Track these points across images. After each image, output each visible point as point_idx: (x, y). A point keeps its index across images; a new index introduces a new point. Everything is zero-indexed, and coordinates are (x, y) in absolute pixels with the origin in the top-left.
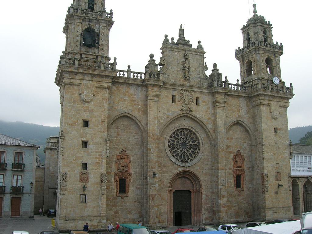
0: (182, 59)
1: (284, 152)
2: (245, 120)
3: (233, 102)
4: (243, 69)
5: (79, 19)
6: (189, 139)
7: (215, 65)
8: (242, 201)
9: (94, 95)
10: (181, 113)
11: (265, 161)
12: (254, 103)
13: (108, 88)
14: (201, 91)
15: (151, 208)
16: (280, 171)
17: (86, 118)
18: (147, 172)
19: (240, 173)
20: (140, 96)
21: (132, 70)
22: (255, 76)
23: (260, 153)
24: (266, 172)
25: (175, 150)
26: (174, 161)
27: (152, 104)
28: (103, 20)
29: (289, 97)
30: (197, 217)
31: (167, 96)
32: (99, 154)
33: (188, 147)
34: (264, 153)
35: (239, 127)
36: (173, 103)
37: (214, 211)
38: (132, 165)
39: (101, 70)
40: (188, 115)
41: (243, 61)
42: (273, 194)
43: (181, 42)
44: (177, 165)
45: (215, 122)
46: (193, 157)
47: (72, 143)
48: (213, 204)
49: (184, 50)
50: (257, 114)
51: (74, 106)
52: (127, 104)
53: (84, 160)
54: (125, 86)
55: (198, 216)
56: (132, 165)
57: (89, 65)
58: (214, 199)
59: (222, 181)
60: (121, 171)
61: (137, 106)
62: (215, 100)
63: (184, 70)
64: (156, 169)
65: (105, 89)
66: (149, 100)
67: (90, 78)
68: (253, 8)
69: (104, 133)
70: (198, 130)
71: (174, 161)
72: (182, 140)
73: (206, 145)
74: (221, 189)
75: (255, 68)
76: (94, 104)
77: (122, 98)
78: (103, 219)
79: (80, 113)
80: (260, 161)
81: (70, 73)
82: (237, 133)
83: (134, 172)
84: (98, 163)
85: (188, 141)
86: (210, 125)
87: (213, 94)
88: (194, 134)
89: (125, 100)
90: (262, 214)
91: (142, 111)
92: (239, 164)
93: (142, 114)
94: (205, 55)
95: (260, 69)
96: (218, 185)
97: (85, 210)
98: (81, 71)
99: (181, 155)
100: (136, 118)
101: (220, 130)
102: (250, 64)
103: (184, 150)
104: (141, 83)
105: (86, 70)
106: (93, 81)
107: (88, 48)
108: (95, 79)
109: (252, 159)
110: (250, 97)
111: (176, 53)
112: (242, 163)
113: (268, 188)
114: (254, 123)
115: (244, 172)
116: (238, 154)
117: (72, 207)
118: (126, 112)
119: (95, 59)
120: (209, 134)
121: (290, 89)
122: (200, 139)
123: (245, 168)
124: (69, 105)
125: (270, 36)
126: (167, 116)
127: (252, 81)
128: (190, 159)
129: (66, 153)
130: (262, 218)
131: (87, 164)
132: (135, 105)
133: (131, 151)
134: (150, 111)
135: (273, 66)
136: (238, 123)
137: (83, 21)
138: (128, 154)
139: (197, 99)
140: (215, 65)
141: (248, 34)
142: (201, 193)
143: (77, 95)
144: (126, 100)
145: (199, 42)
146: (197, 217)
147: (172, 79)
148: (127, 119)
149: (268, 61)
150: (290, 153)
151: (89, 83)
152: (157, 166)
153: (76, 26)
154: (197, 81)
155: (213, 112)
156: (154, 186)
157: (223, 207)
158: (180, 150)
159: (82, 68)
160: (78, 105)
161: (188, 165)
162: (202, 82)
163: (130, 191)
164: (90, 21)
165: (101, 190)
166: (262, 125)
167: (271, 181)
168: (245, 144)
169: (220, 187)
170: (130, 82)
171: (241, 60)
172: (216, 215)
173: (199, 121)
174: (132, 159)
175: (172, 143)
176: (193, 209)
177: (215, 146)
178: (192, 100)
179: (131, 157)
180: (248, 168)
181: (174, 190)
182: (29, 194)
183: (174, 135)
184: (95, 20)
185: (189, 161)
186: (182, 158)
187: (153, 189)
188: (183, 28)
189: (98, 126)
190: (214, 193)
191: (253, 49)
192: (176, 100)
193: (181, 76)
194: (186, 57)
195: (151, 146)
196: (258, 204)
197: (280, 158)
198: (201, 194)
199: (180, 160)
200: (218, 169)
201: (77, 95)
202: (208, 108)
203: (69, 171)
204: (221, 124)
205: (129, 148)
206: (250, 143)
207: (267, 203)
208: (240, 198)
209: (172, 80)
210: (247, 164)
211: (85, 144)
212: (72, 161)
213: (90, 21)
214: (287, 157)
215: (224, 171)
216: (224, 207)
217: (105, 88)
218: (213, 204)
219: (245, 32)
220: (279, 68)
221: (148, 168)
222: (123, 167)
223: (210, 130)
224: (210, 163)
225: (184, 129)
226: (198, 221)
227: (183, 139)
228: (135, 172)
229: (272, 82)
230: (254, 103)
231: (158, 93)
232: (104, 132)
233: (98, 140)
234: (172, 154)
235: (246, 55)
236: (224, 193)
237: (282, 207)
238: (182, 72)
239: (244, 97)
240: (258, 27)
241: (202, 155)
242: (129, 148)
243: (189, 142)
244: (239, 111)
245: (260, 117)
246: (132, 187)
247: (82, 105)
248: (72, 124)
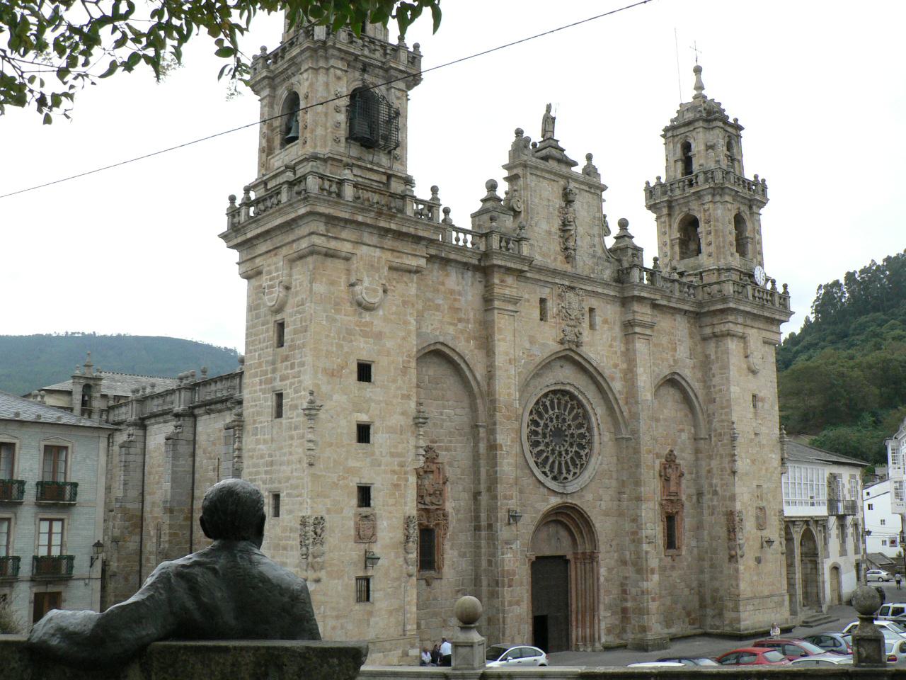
0: (559, 202)
1: (771, 458)
2: (689, 373)
3: (662, 324)
4: (670, 236)
5: (342, 59)
6: (569, 418)
7: (623, 224)
8: (678, 581)
9: (385, 291)
10: (558, 347)
11: (736, 478)
12: (708, 331)
13: (417, 271)
14: (600, 290)
15: (507, 608)
16: (764, 504)
17: (365, 357)
18: (493, 510)
19: (674, 511)
20: (470, 298)
21: (456, 223)
22: (712, 260)
23: (722, 457)
24: (738, 506)
25: (540, 448)
26: (541, 477)
27: (502, 321)
28: (401, 71)
29: (783, 318)
30: (584, 627)
31: (528, 301)
32: (401, 459)
33: (566, 441)
34: (736, 458)
35: (672, 391)
36: (541, 320)
37: (624, 610)
38: (448, 488)
39: (408, 220)
40: (572, 354)
41: (669, 215)
42: (752, 563)
43: (554, 152)
44: (546, 489)
45: (630, 375)
46: (579, 467)
47: (333, 428)
48: (624, 592)
49: (563, 177)
50: (713, 357)
51: (335, 320)
52: (443, 317)
53: (363, 477)
54: (436, 266)
55: (588, 624)
56: (449, 489)
57: (377, 203)
58: (626, 578)
59: (649, 532)
60: (427, 507)
61: (464, 325)
62: (630, 318)
63: (564, 231)
64: (514, 501)
65: (408, 274)
66: (496, 311)
67: (374, 240)
68: (692, 78)
69: (410, 399)
70: (589, 395)
71: (541, 477)
72: (555, 420)
73: (607, 437)
74: (647, 553)
75: (711, 238)
76: (384, 314)
77: (429, 300)
78: (413, 646)
79: (351, 341)
80: (722, 479)
81: (331, 220)
82: (670, 407)
83: (453, 508)
84: (396, 486)
85: (566, 424)
87: (625, 302)
88: (580, 405)
89: (438, 308)
90: (729, 615)
91: (475, 338)
92: (673, 489)
93: (476, 348)
94: (604, 195)
95: (724, 241)
96: (637, 541)
97: (368, 620)
98: (360, 219)
99: (553, 462)
100: (462, 357)
101: (644, 398)
102: (690, 225)
103: (560, 447)
104: (477, 263)
105: (372, 215)
106: (383, 248)
107: (364, 149)
108: (388, 243)
109: (697, 473)
110: (697, 314)
111: (545, 183)
112: (679, 484)
113: (744, 548)
114: (706, 380)
115: (683, 505)
116: (670, 460)
117: (337, 617)
118: (441, 341)
119: (381, 185)
120: (616, 406)
121: (785, 299)
122: (593, 419)
123: (684, 498)
124: (325, 315)
125: (739, 158)
126: (531, 356)
127: (701, 273)
128: (572, 473)
129: (319, 458)
130: (727, 625)
131: (372, 490)
132: (460, 320)
133: (447, 449)
134: (499, 340)
135: (747, 238)
136: (673, 381)
137: (348, 65)
138: (440, 460)
139: (591, 310)
140: (623, 224)
141: (687, 147)
142: (595, 564)
143: (343, 287)
144: (440, 305)
145: (589, 157)
146: (584, 627)
147: (540, 254)
148: (435, 360)
149: (739, 221)
150: (782, 459)
151: (373, 254)
152: (514, 492)
153: (332, 79)
154: (590, 262)
155: (623, 349)
156: (511, 548)
157: (652, 598)
158: (551, 448)
159: (363, 210)
160: (347, 317)
161: (571, 487)
162: (600, 268)
163: (447, 563)
164: (364, 70)
165: (407, 563)
166: (728, 389)
167: (748, 530)
168: (683, 434)
169: (645, 547)
170: (452, 256)
171: (665, 211)
172: (633, 622)
173: (595, 374)
174: (449, 472)
175: (533, 428)
176: (574, 606)
177: (628, 439)
178: (583, 315)
179: (447, 467)
180: (689, 496)
181: (534, 559)
182: (87, 581)
183: (539, 410)
184: (381, 68)
185: (570, 477)
186: (556, 470)
187: (509, 555)
188: (552, 114)
189: (394, 381)
190: (624, 563)
191: (710, 188)
192: (549, 312)
193: (558, 248)
194: (571, 198)
195: (502, 437)
196: (717, 590)
197: (764, 472)
198: (595, 567)
199: (550, 476)
200: (639, 499)
201: (342, 288)
202: (614, 339)
203: (328, 511)
204: (645, 381)
205: (441, 441)
206: (693, 431)
207: (743, 586)
208: (675, 574)
209: (538, 259)
210: (688, 487)
211: (363, 433)
212: (334, 483)
213: (364, 70)
214: (776, 468)
215: (651, 505)
216: (654, 600)
217: (410, 272)
218: (624, 592)
219: (676, 139)
220: (760, 243)
221: (495, 498)
222: (430, 495)
223: (618, 396)
224: (614, 483)
225: (559, 390)
226: (588, 639)
228: (457, 511)
229: (751, 276)
230: (708, 331)
231: (514, 292)
232: (408, 397)
233: (397, 420)
235: (682, 201)
236: (654, 562)
237: (768, 597)
238: (560, 237)
239: (686, 312)
240: (717, 131)
241: (599, 462)
242: (441, 441)
243: (569, 425)
244: (676, 351)
245: (725, 367)
246: (450, 552)
247: (356, 318)
248: (333, 373)
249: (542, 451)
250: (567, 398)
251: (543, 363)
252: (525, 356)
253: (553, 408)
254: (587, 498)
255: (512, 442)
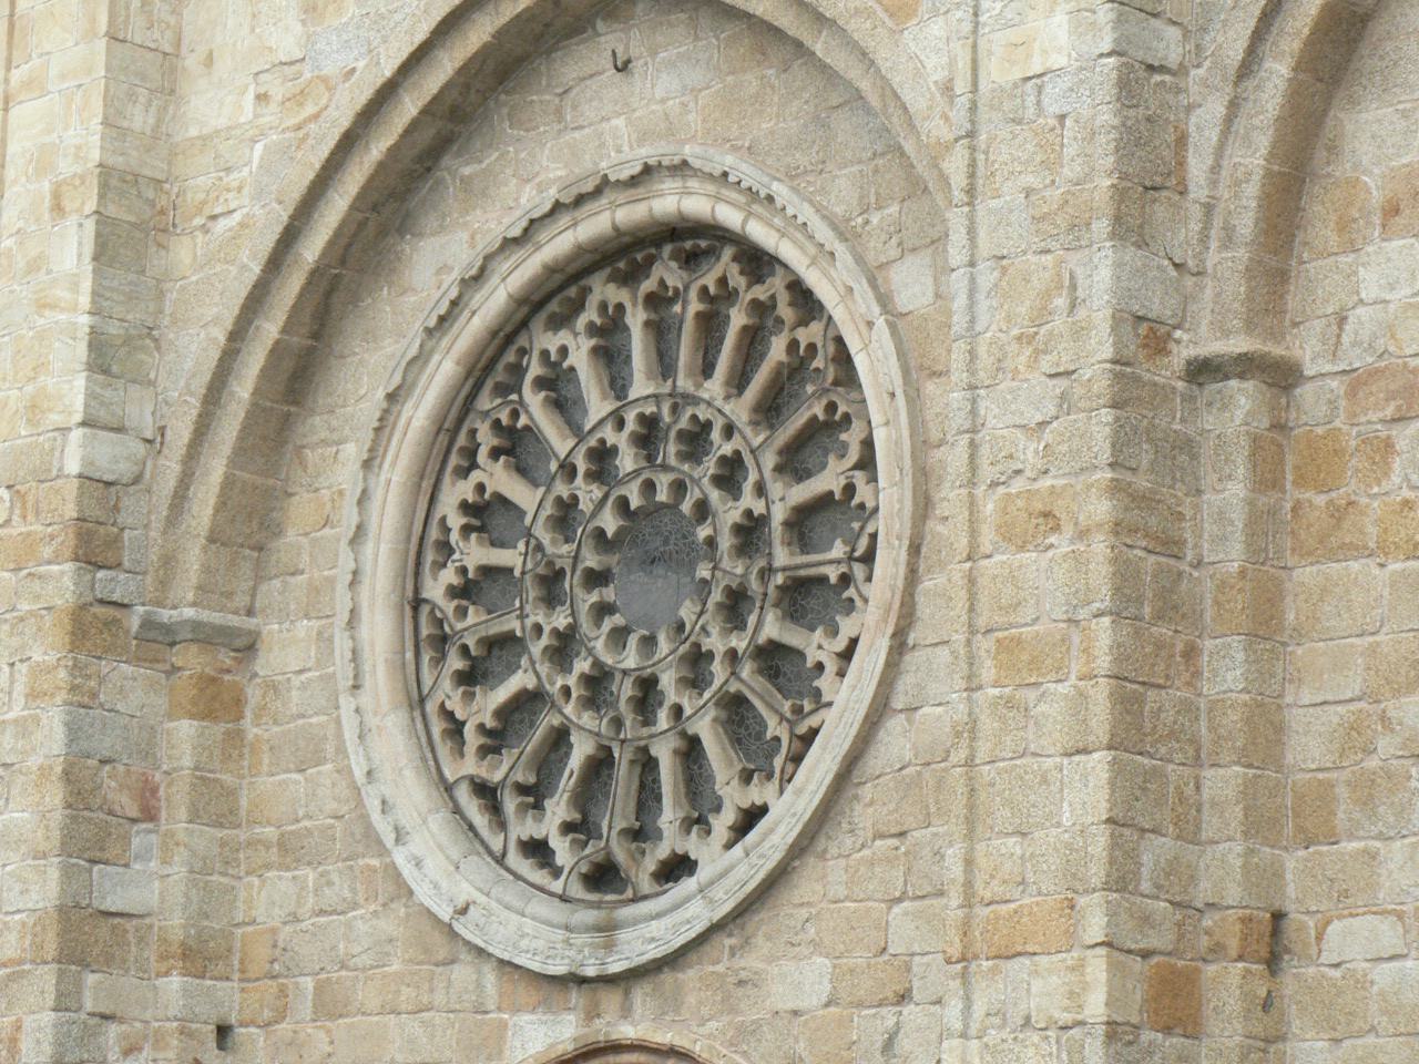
72: (627, 461)
86: (937, 28)
99: (600, 765)
128: (723, 822)
158: (582, 666)
227: (649, 436)
234: (471, 766)
243: (730, 475)
249: (528, 702)
250: (726, 265)
251: (409, 106)
252: (270, 115)
253: (617, 385)
254: (780, 996)
255: (33, 695)
